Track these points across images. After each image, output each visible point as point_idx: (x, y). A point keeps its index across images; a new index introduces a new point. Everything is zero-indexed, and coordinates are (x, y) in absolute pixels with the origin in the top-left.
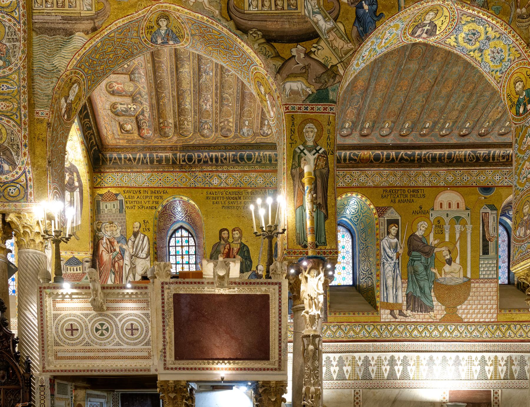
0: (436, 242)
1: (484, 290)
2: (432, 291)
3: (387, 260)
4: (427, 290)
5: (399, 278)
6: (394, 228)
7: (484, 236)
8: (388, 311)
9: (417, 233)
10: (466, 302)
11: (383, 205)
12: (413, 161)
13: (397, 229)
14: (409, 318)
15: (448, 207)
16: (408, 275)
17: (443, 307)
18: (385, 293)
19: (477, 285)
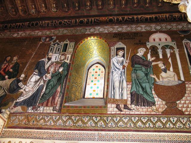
0: (153, 59)
3: (115, 70)
4: (148, 90)
6: (121, 52)
8: (114, 106)
9: (138, 54)
10: (184, 98)
14: (134, 111)
15: (159, 40)
17: (164, 102)
18: (113, 92)
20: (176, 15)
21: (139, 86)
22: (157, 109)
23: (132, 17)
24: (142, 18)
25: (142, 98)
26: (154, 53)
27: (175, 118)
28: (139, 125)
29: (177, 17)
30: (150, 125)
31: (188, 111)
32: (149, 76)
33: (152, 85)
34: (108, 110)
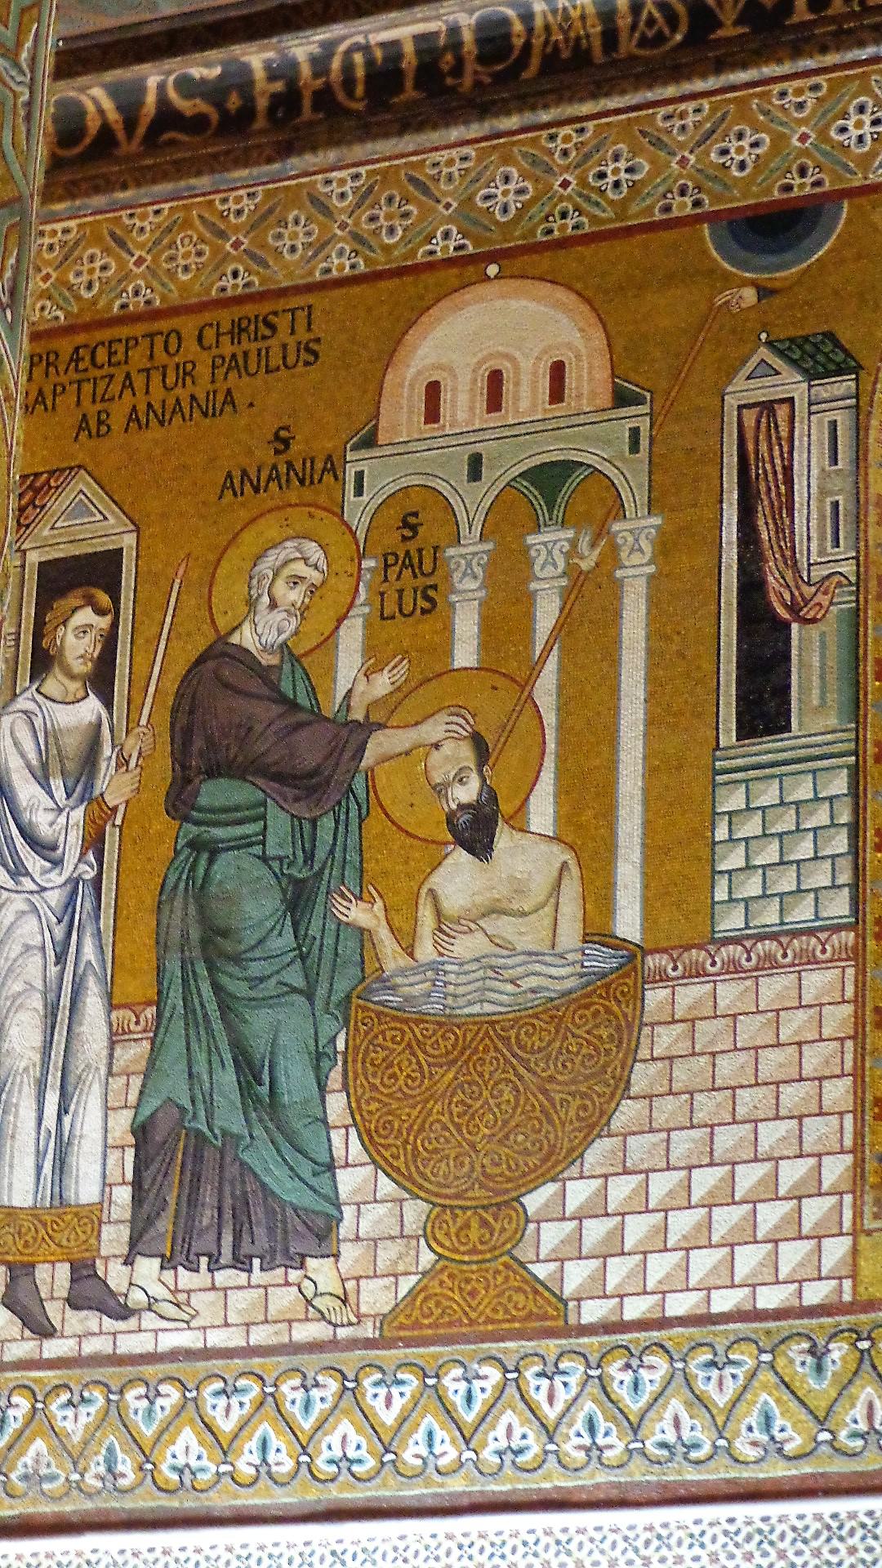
1: (750, 1030)
2: (335, 1078)
5: (94, 1003)
6: (86, 616)
7: (752, 587)
9: (246, 638)
10: (597, 1153)
13: (104, 622)
14: (149, 1320)
15: (481, 404)
16: (160, 971)
17: (415, 1212)
19: (690, 995)
21: (212, 1050)
22: (351, 1285)
24: (336, 64)
25: (227, 1175)
26: (401, 592)
27: (485, 1370)
28: (181, 1461)
30: (272, 1457)
32: (319, 909)
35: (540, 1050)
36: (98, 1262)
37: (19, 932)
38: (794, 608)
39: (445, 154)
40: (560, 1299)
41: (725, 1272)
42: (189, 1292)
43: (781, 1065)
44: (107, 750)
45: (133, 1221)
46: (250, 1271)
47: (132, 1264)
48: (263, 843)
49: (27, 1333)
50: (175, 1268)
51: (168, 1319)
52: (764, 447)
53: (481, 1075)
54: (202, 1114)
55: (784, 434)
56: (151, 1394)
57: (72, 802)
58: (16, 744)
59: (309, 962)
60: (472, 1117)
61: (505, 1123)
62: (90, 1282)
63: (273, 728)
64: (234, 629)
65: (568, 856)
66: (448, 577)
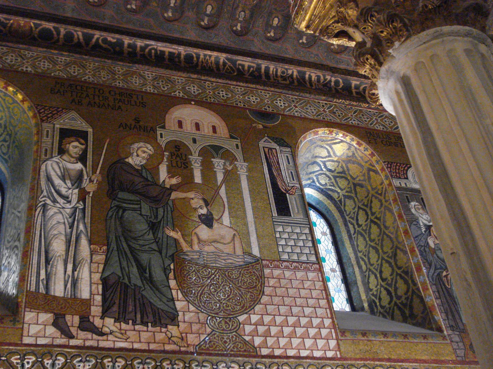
0: (174, 181)
2: (171, 275)
3: (55, 201)
4: (158, 274)
5: (84, 242)
6: (76, 144)
8: (46, 317)
9: (130, 160)
10: (258, 308)
11: (54, 104)
12: (121, 53)
13: (83, 147)
14: (110, 337)
15: (194, 128)
16: (108, 238)
19: (277, 272)
20: (246, 64)
22: (184, 335)
23: (117, 39)
24: (147, 50)
25: (137, 297)
26: (177, 162)
29: (246, 68)
31: (269, 344)
32: (161, 231)
33: (169, 262)
34: (25, 333)
35: (235, 279)
36: (90, 317)
37: (55, 217)
38: (285, 190)
39: (176, 78)
40: (254, 346)
41: (302, 345)
42: (126, 330)
43: (306, 294)
44: (85, 177)
45: (103, 306)
46: (148, 327)
47: (103, 319)
48: (141, 211)
49: (63, 336)
50: (120, 322)
51: (119, 338)
52: (271, 156)
53: (219, 282)
54: (126, 278)
55: (276, 155)
56: (114, 361)
57: (74, 187)
58: (53, 169)
59: (158, 244)
60: (218, 293)
61: (228, 296)
62: (87, 323)
63: (142, 183)
64: (126, 158)
65: (235, 232)
66: (190, 162)
